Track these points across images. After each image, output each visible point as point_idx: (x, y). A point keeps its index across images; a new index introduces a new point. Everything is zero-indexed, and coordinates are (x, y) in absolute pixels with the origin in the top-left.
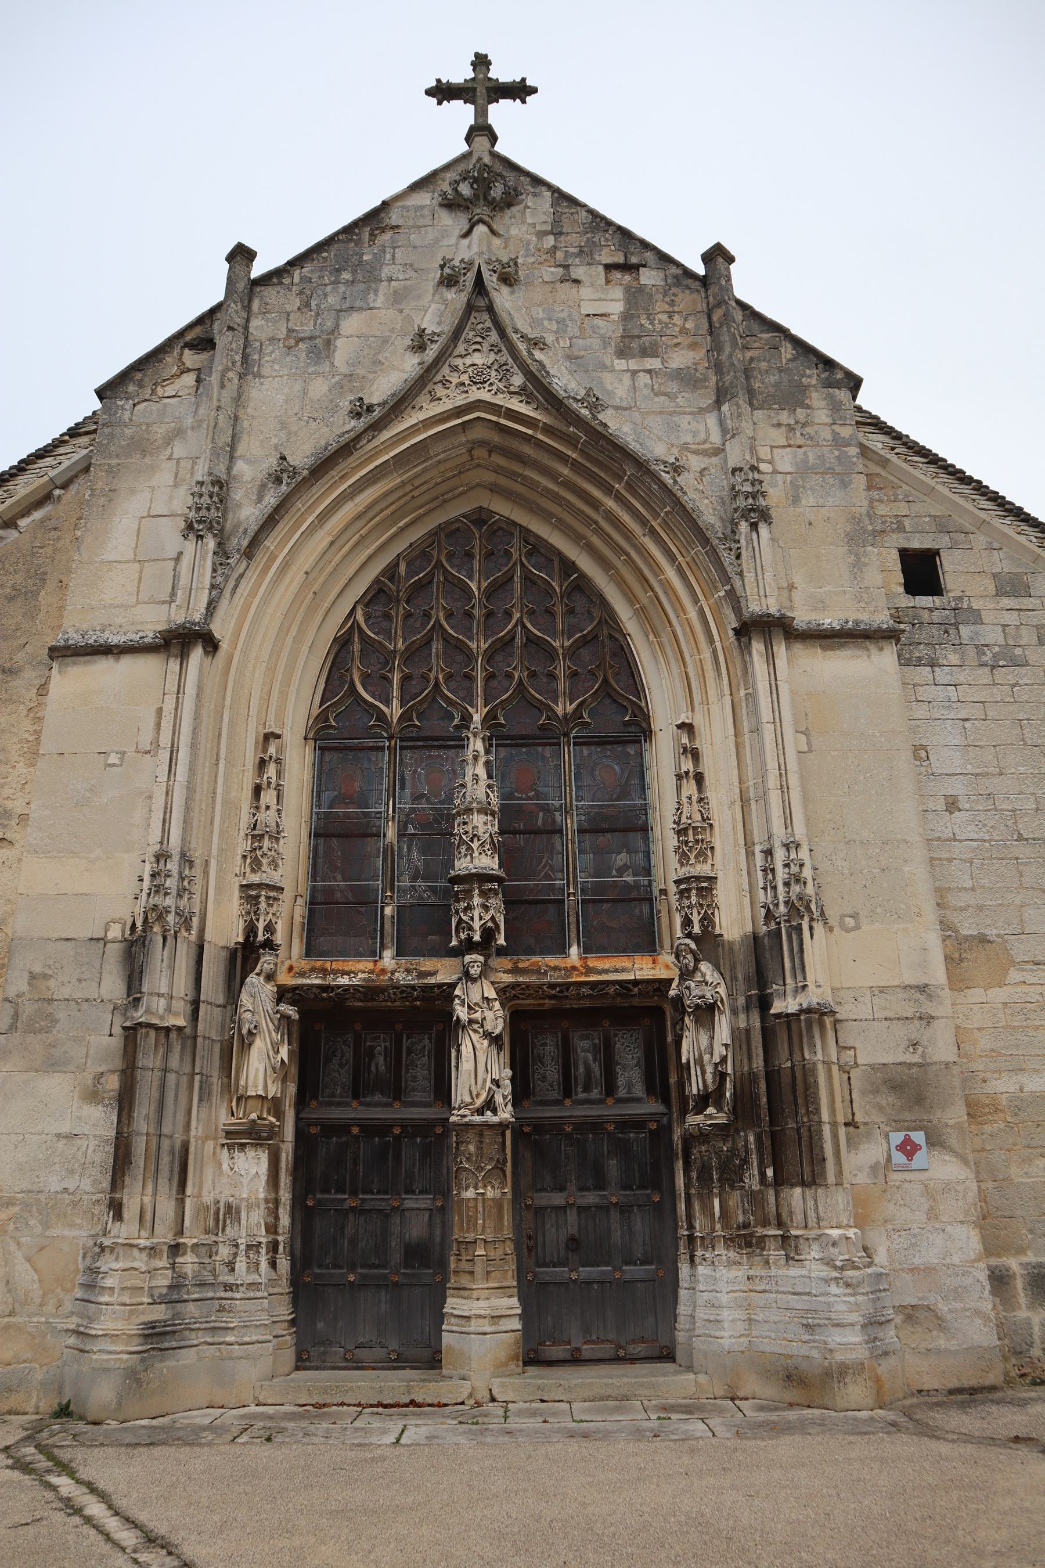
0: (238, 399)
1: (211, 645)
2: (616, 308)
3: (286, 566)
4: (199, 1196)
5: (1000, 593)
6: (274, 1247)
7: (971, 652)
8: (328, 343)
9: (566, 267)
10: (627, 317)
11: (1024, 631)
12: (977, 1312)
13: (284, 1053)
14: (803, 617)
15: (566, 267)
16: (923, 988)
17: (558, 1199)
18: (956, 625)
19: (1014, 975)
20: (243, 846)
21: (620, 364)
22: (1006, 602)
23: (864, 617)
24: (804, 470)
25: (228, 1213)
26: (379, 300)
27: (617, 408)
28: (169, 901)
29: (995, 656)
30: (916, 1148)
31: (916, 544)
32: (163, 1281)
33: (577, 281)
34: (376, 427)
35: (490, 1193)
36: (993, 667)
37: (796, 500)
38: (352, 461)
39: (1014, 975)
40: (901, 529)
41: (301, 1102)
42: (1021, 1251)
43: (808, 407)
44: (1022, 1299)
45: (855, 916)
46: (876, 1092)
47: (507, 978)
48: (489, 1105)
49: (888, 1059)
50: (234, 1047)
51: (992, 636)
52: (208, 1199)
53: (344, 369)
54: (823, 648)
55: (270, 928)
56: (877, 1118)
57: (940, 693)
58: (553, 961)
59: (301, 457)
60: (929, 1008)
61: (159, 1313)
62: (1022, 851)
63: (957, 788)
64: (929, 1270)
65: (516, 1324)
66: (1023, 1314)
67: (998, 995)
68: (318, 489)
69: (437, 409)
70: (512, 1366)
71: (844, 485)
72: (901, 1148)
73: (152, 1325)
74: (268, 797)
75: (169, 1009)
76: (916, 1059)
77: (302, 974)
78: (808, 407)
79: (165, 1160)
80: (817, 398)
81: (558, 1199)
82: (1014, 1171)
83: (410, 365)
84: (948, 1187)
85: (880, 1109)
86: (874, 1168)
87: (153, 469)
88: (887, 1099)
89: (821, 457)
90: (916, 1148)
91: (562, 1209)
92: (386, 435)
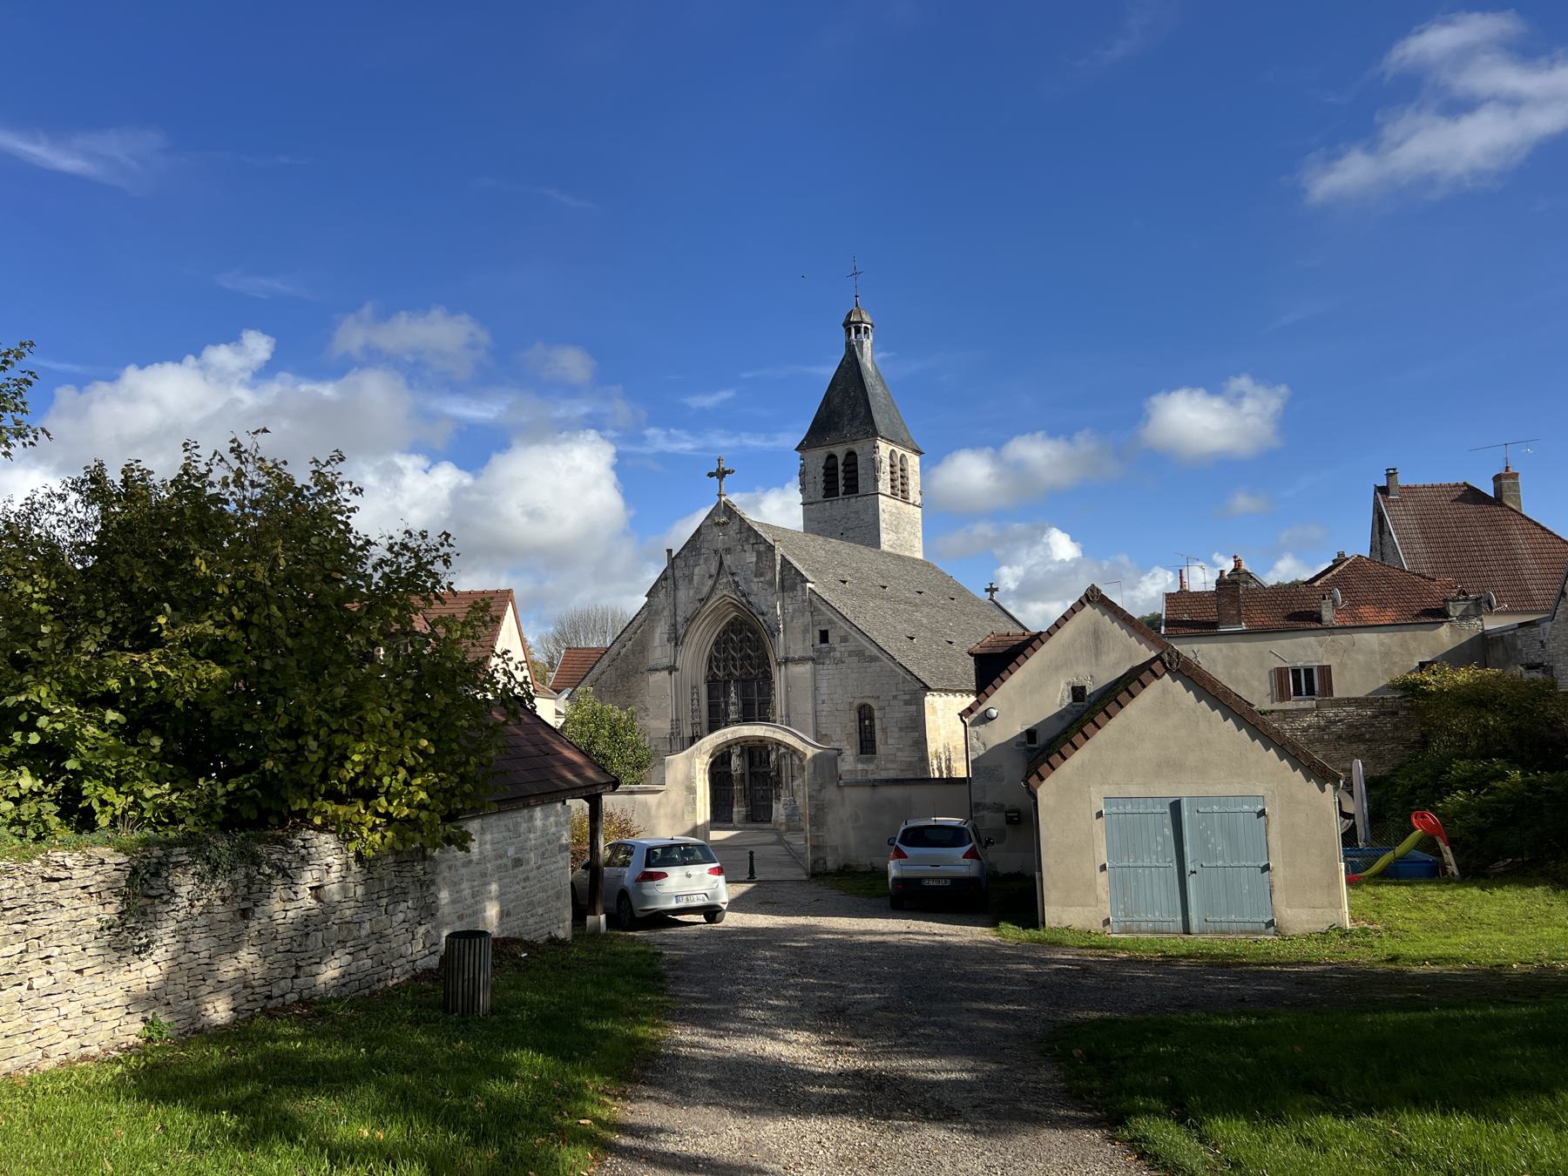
51: (838, 654)
83: (710, 583)
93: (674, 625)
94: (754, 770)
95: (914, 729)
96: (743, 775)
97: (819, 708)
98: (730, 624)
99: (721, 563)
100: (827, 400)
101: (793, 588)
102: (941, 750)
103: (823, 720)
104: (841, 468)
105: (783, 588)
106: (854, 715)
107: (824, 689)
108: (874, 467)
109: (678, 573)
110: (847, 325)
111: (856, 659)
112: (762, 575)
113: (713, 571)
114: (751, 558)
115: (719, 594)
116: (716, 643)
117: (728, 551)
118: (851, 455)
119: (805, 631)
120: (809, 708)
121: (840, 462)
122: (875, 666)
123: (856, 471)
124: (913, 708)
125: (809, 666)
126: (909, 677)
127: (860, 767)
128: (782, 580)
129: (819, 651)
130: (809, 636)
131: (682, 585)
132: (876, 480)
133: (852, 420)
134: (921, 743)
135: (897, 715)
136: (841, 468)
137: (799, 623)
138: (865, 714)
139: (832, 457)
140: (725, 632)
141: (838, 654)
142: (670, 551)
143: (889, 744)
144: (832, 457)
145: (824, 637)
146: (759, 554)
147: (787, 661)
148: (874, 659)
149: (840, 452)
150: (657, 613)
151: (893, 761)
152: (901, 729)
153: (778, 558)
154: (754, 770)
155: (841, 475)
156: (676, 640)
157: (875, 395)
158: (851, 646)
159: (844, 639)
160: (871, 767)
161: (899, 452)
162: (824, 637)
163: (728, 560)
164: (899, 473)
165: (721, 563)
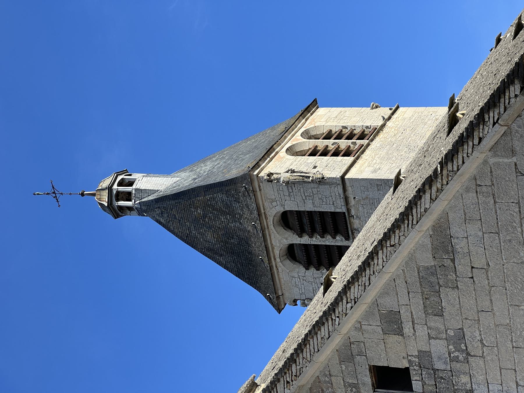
5: (400, 332)
7: (457, 366)
11: (432, 324)
18: (435, 370)
22: (407, 329)
29: (457, 350)
31: (367, 379)
36: (468, 354)
104: (305, 240)
108: (300, 183)
110: (119, 213)
111: (449, 297)
118: (287, 220)
121: (296, 240)
122: (467, 238)
123: (310, 213)
126: (492, 134)
132: (322, 181)
133: (232, 214)
136: (305, 240)
139: (291, 252)
141: (439, 348)
144: (291, 252)
148: (443, 242)
149: (281, 239)
155: (317, 240)
157: (211, 173)
158: (410, 307)
159: (392, 323)
161: (296, 139)
164: (330, 142)
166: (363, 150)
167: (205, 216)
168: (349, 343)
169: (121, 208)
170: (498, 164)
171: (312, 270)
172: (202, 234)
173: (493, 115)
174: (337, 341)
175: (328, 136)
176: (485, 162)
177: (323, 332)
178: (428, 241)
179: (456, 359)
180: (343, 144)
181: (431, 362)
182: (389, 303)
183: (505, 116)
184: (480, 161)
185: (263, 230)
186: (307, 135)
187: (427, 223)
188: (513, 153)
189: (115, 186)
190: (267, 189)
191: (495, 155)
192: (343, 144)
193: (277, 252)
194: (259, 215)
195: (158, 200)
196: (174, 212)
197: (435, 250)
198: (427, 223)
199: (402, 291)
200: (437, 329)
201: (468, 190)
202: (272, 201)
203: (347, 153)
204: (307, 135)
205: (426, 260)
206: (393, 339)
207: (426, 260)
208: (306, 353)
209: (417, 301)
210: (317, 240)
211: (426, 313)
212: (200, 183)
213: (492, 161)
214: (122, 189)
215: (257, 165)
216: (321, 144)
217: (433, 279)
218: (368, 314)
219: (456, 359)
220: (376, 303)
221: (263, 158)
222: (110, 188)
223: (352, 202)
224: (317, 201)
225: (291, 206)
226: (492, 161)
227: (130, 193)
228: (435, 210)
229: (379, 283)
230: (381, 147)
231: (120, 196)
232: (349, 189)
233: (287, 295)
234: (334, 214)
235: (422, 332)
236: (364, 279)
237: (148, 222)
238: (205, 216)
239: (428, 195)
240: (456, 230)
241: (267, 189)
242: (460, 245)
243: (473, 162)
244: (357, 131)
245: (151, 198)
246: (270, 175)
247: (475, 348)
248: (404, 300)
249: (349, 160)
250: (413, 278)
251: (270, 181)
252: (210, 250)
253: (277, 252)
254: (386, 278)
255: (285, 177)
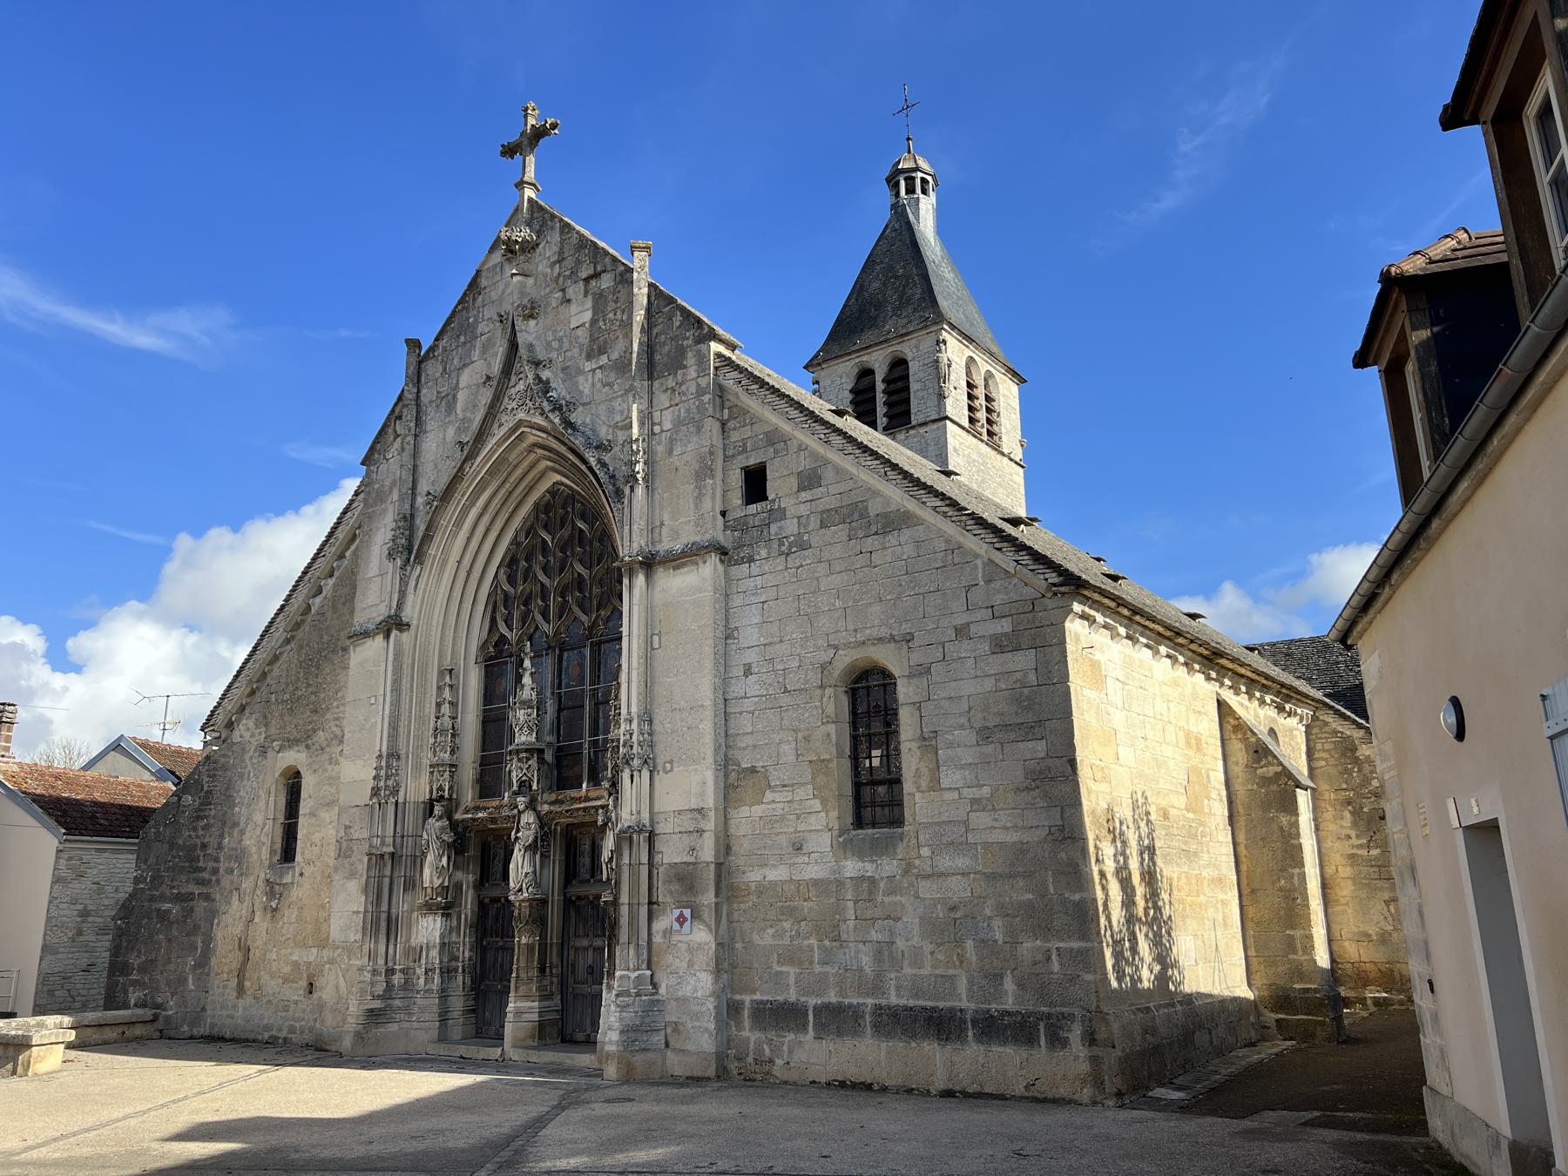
0: (415, 455)
1: (402, 626)
2: (587, 316)
3: (444, 562)
4: (408, 940)
5: (801, 489)
6: (447, 972)
7: (775, 545)
8: (454, 396)
9: (563, 290)
10: (594, 322)
12: (706, 1030)
13: (445, 860)
14: (666, 545)
15: (563, 290)
16: (700, 811)
17: (585, 943)
19: (769, 796)
20: (432, 740)
21: (588, 366)
22: (804, 495)
23: (698, 539)
24: (678, 423)
25: (416, 954)
26: (476, 355)
27: (584, 404)
28: (382, 784)
30: (685, 919)
31: (753, 461)
32: (380, 988)
33: (569, 301)
34: (470, 457)
35: (524, 940)
37: (670, 452)
38: (464, 484)
39: (769, 796)
40: (745, 450)
41: (479, 885)
42: (753, 992)
43: (685, 367)
44: (747, 1024)
45: (671, 762)
46: (670, 882)
47: (546, 808)
48: (520, 890)
49: (678, 860)
50: (418, 860)
52: (413, 942)
53: (461, 416)
54: (675, 568)
55: (441, 789)
56: (669, 899)
57: (750, 583)
58: (573, 793)
59: (440, 488)
60: (702, 825)
61: (377, 1004)
62: (785, 700)
63: (751, 657)
64: (685, 1000)
65: (535, 1017)
66: (746, 1033)
67: (758, 810)
68: (451, 508)
69: (504, 429)
70: (530, 1042)
71: (699, 429)
72: (678, 920)
73: (372, 1010)
74: (446, 709)
75: (383, 843)
76: (692, 860)
77: (467, 812)
78: (685, 367)
79: (383, 925)
80: (690, 360)
81: (585, 943)
82: (755, 936)
84: (700, 946)
85: (671, 893)
86: (665, 932)
87: (385, 510)
88: (675, 887)
89: (688, 411)
90: (685, 919)
91: (586, 949)
92: (479, 459)
93: (408, 520)
94: (576, 890)
95: (1029, 731)
96: (540, 904)
97: (737, 689)
98: (542, 508)
99: (513, 346)
100: (859, 288)
101: (677, 364)
102: (1124, 812)
103: (744, 724)
104: (880, 386)
105: (651, 369)
106: (835, 703)
107: (750, 635)
108: (938, 374)
109: (427, 394)
111: (839, 532)
112: (602, 351)
113: (496, 367)
114: (580, 313)
115: (507, 421)
116: (511, 562)
117: (531, 312)
118: (899, 364)
119: (704, 471)
120: (705, 690)
121: (879, 377)
122: (901, 544)
124: (1024, 661)
125: (708, 570)
126: (1006, 560)
127: (851, 867)
128: (649, 348)
129: (741, 526)
130: (713, 485)
131: (432, 423)
132: (942, 397)
133: (899, 308)
134: (1056, 777)
135: (968, 688)
136: (880, 386)
137: (687, 452)
138: (870, 702)
139: (866, 373)
140: (529, 530)
141: (791, 527)
142: (413, 344)
143: (945, 783)
144: (866, 373)
145: (755, 484)
146: (599, 301)
147: (649, 563)
148: (894, 522)
149: (878, 361)
150: (381, 497)
151: (956, 846)
152: (985, 735)
153: (641, 294)
154: (576, 890)
155: (880, 398)
156: (411, 549)
157: (942, 278)
158: (828, 496)
159: (809, 480)
160: (888, 867)
161: (984, 365)
162: (755, 484)
163: (529, 333)
165: (513, 346)
166: (978, 435)
167: (896, 277)
168: (785, 439)
169: (897, 184)
170: (976, 568)
171: (851, 397)
172: (876, 277)
173: (1026, 559)
174: (786, 427)
175: (988, 399)
176: (977, 556)
177: (794, 413)
178: (893, 508)
179: (781, 544)
180: (982, 415)
181: (776, 520)
182: (828, 475)
183: (1025, 571)
184: (978, 550)
185: (886, 341)
186: (989, 377)
187: (911, 506)
188: (988, 582)
189: (920, 175)
190: (930, 341)
191: (985, 565)
192: (982, 415)
193: (865, 358)
194: (902, 335)
195: (908, 223)
196: (898, 244)
197: (885, 515)
198: (911, 506)
199: (842, 487)
200: (808, 524)
201: (948, 541)
202: (917, 347)
203: (972, 420)
204: (989, 377)
205: (874, 508)
206: (794, 482)
207: (874, 508)
208: (771, 398)
209: (833, 503)
210: (880, 398)
211: (822, 512)
212: (931, 268)
213: (979, 562)
214: (918, 182)
215: (953, 327)
216: (980, 392)
217: (856, 516)
218: (814, 455)
219: (781, 544)
220: (827, 462)
221: (961, 333)
222: (917, 169)
223: (922, 430)
224: (920, 394)
225: (913, 367)
226: (979, 562)
227: (913, 192)
228: (925, 512)
229: (847, 464)
230: (981, 455)
231: (910, 182)
232: (935, 426)
233: (823, 373)
234: (908, 413)
235: (804, 510)
236: (850, 448)
237: (887, 215)
238: (896, 277)
239: (939, 503)
240: (906, 534)
241: (930, 341)
242: (892, 539)
243: (977, 545)
244: (995, 428)
245: (911, 216)
246: (944, 342)
247: (794, 560)
248: (833, 489)
249: (966, 423)
250: (856, 497)
251: (938, 343)
252: (862, 286)
253: (865, 358)
254: (853, 470)
255: (944, 357)
